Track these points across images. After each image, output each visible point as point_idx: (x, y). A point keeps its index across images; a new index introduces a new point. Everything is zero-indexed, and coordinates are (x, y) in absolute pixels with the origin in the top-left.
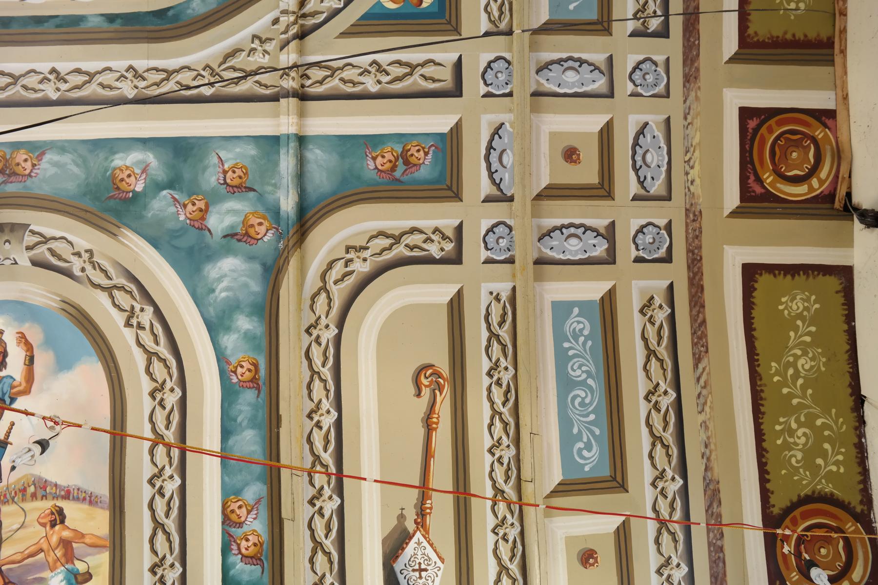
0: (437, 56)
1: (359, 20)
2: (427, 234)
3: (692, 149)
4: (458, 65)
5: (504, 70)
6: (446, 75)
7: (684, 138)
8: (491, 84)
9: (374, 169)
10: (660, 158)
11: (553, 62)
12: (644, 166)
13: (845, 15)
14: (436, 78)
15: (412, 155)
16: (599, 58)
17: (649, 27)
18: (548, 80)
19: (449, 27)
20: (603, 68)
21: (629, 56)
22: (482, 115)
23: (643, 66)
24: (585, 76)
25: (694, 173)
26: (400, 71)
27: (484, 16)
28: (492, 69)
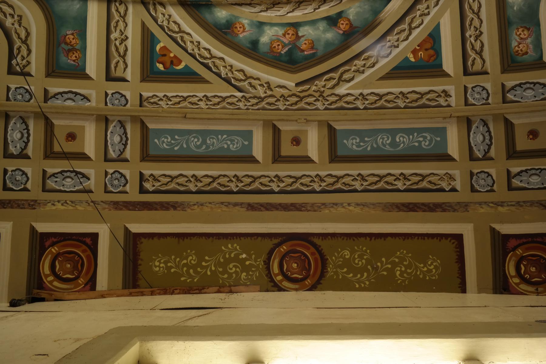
0: (129, 70)
1: (151, 32)
2: (27, 57)
3: (73, 205)
4: (124, 80)
5: (120, 103)
6: (119, 73)
7: (80, 201)
8: (113, 96)
9: (66, 34)
10: (68, 186)
11: (125, 130)
12: (63, 177)
13: (152, 295)
14: (117, 69)
15: (74, 54)
16: (128, 154)
17: (145, 183)
18: (115, 126)
19: (145, 76)
20: (122, 156)
21: (129, 171)
22: (95, 91)
23: (123, 179)
24: (117, 147)
25: (59, 206)
26: (122, 50)
27: (151, 94)
28: (121, 97)
